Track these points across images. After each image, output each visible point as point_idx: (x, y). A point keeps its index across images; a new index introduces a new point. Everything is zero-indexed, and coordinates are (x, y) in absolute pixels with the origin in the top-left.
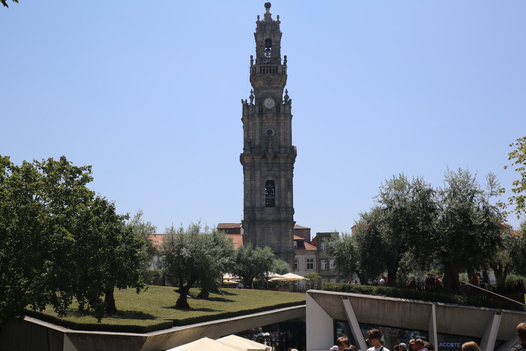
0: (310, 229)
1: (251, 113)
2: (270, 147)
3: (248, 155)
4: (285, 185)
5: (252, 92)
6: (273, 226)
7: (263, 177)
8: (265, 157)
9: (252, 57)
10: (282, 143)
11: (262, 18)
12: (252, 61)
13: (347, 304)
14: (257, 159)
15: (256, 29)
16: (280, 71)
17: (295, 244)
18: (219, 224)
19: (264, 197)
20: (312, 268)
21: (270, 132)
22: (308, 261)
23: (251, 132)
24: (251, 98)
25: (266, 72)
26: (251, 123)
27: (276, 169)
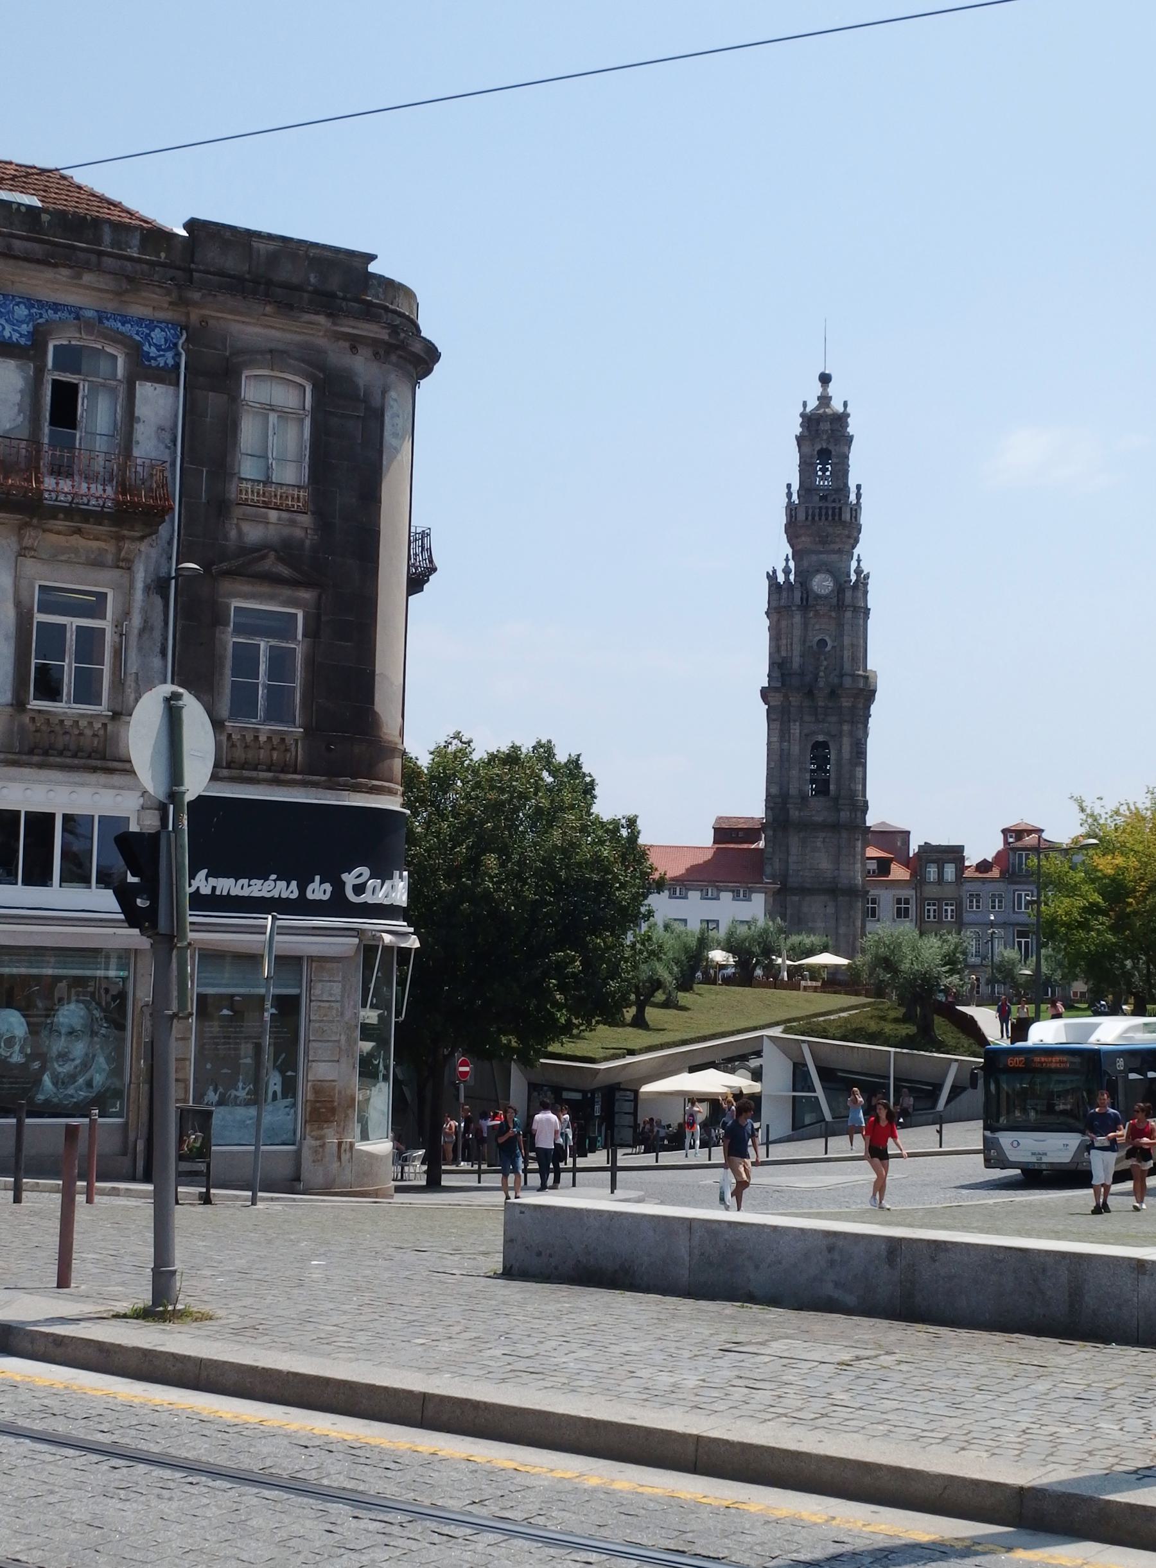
0: (908, 833)
1: (788, 602)
2: (822, 674)
3: (776, 690)
4: (851, 753)
5: (787, 560)
6: (824, 835)
7: (807, 735)
8: (810, 694)
9: (789, 486)
10: (847, 667)
11: (813, 404)
12: (789, 495)
13: (805, 1048)
14: (795, 700)
15: (801, 425)
16: (846, 516)
17: (872, 865)
18: (720, 819)
19: (808, 776)
20: (906, 916)
21: (822, 643)
22: (899, 901)
23: (784, 642)
24: (787, 571)
25: (817, 518)
26: (784, 623)
27: (833, 719)
